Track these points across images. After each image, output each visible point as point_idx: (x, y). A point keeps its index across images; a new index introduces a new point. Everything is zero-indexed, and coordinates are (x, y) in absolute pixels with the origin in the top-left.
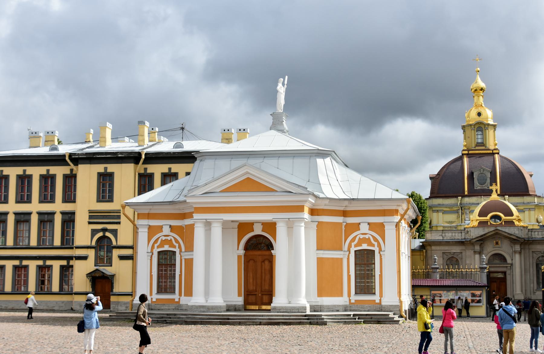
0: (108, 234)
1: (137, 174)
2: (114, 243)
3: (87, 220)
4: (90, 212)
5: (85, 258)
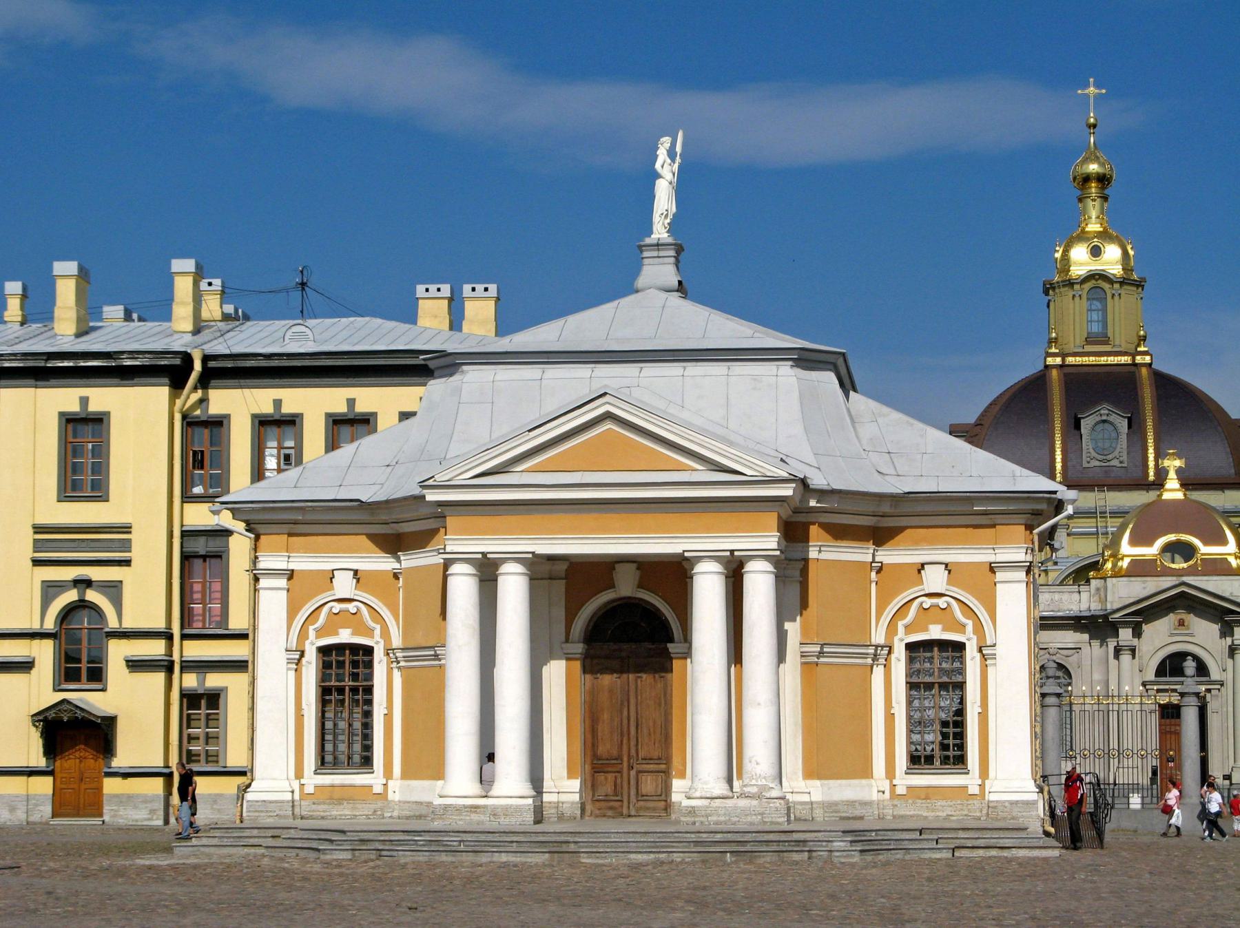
0: (92, 596)
1: (178, 417)
2: (113, 623)
3: (28, 553)
4: (38, 529)
5: (25, 666)
